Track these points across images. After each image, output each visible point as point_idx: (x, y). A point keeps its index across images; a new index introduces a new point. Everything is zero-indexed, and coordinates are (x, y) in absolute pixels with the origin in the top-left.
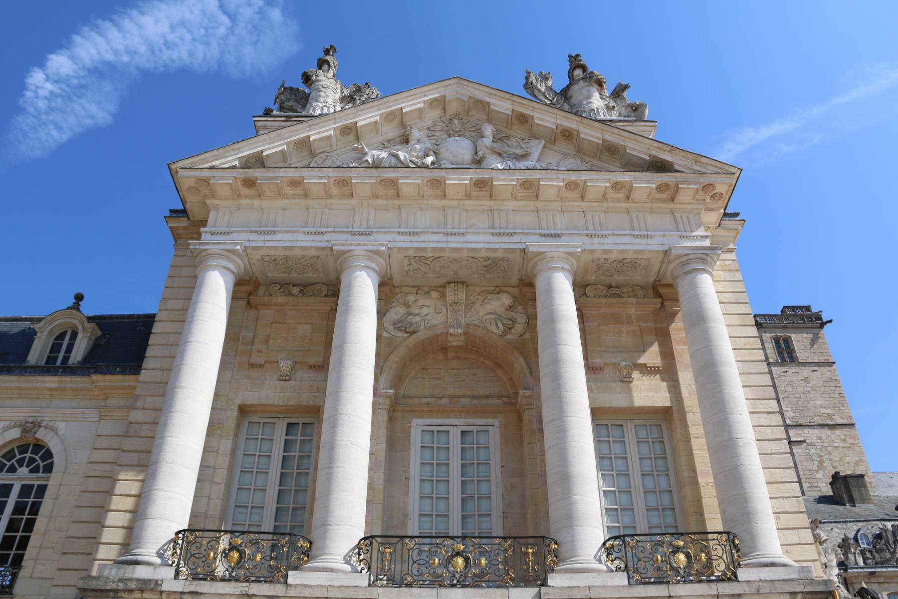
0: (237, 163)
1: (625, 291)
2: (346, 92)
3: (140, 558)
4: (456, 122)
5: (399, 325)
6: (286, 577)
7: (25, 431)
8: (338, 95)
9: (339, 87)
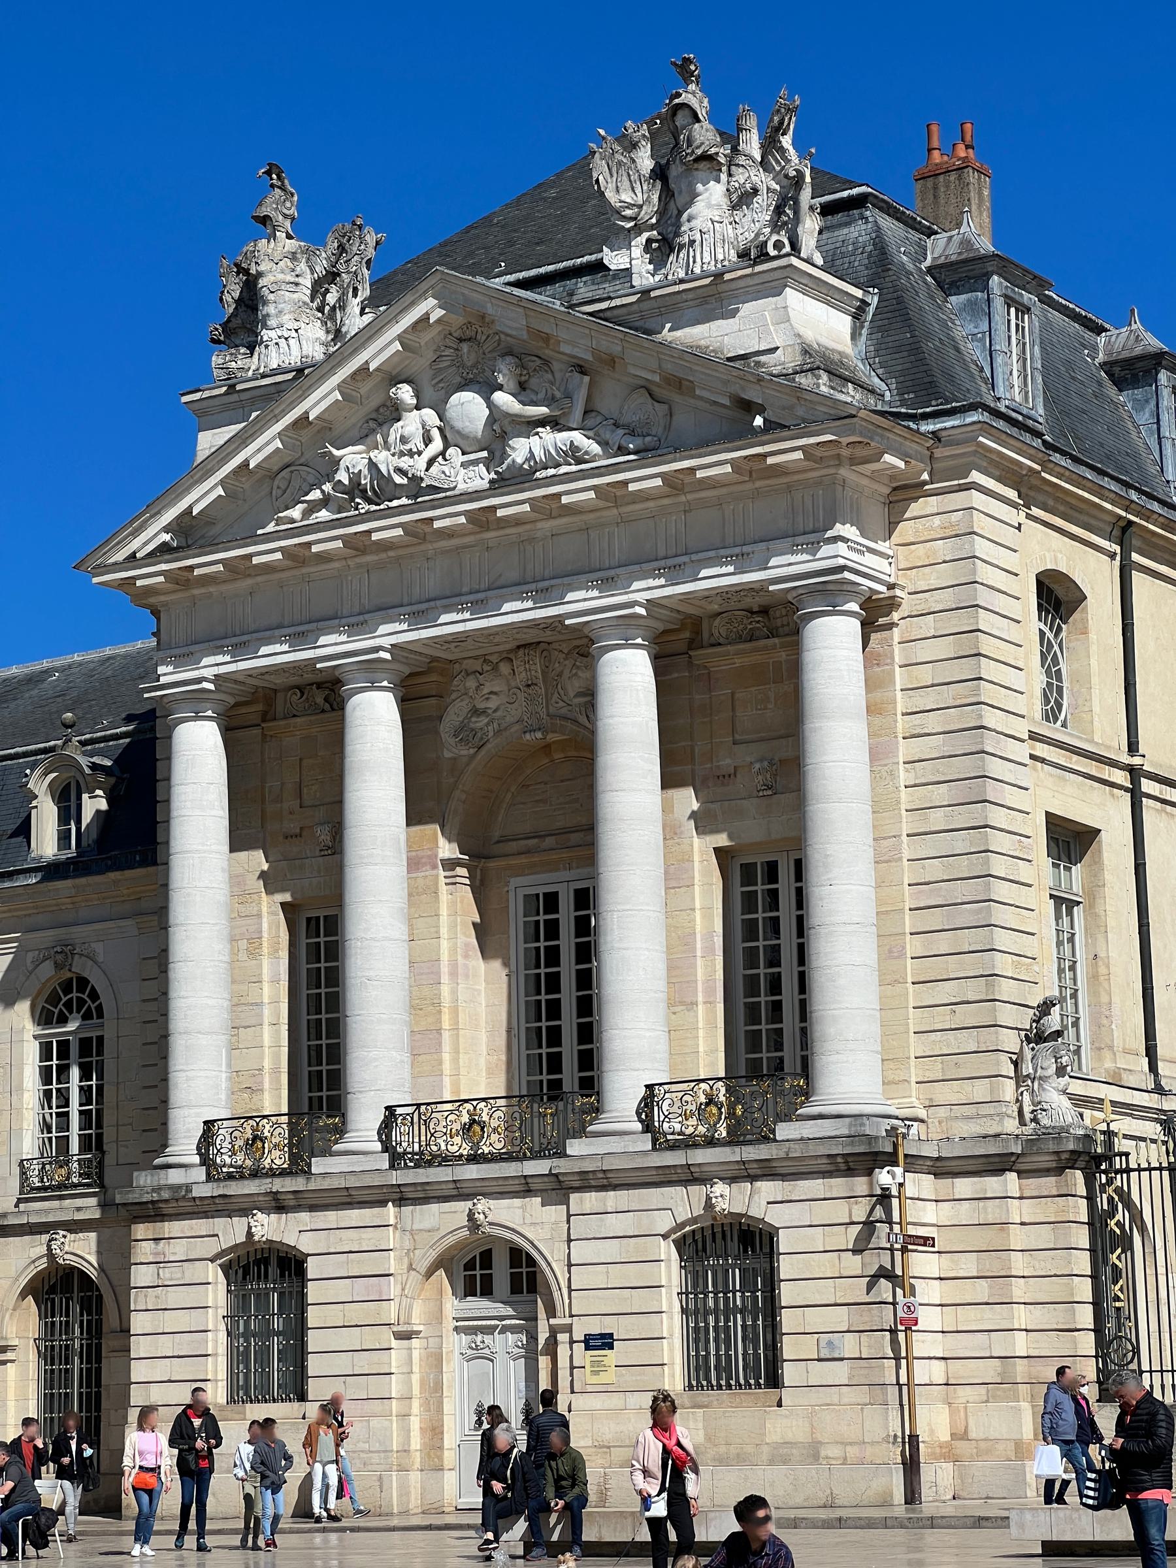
0: (166, 537)
1: (778, 614)
2: (321, 266)
3: (171, 1160)
4: (465, 347)
5: (464, 733)
6: (309, 1165)
7: (58, 966)
8: (307, 281)
9: (302, 266)
